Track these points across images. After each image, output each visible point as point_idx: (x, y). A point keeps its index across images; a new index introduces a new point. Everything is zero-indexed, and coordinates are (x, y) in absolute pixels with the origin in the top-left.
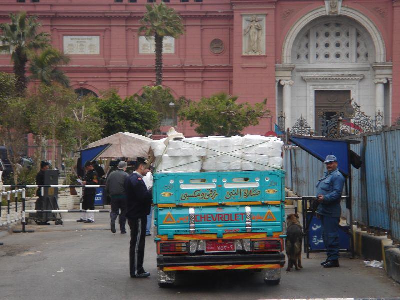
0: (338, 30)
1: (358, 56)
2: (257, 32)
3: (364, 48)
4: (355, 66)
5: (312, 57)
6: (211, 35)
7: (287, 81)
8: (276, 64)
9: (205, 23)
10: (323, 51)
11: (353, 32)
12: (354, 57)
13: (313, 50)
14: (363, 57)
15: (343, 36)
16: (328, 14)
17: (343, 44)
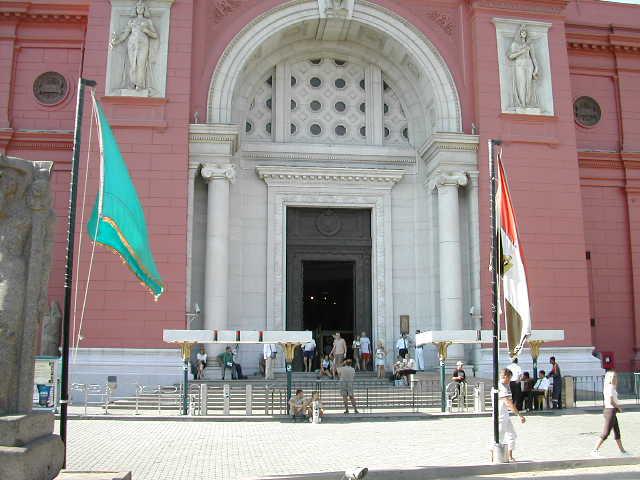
0: (340, 72)
1: (387, 132)
2: (146, 40)
3: (400, 116)
4: (384, 152)
5: (281, 129)
6: (37, 62)
7: (219, 167)
8: (192, 121)
9: (27, 33)
10: (305, 117)
11: (374, 79)
12: (379, 134)
13: (282, 116)
14: (396, 135)
15: (353, 86)
16: (323, 16)
17: (353, 105)
